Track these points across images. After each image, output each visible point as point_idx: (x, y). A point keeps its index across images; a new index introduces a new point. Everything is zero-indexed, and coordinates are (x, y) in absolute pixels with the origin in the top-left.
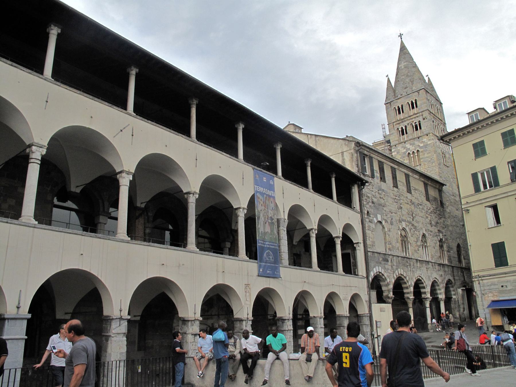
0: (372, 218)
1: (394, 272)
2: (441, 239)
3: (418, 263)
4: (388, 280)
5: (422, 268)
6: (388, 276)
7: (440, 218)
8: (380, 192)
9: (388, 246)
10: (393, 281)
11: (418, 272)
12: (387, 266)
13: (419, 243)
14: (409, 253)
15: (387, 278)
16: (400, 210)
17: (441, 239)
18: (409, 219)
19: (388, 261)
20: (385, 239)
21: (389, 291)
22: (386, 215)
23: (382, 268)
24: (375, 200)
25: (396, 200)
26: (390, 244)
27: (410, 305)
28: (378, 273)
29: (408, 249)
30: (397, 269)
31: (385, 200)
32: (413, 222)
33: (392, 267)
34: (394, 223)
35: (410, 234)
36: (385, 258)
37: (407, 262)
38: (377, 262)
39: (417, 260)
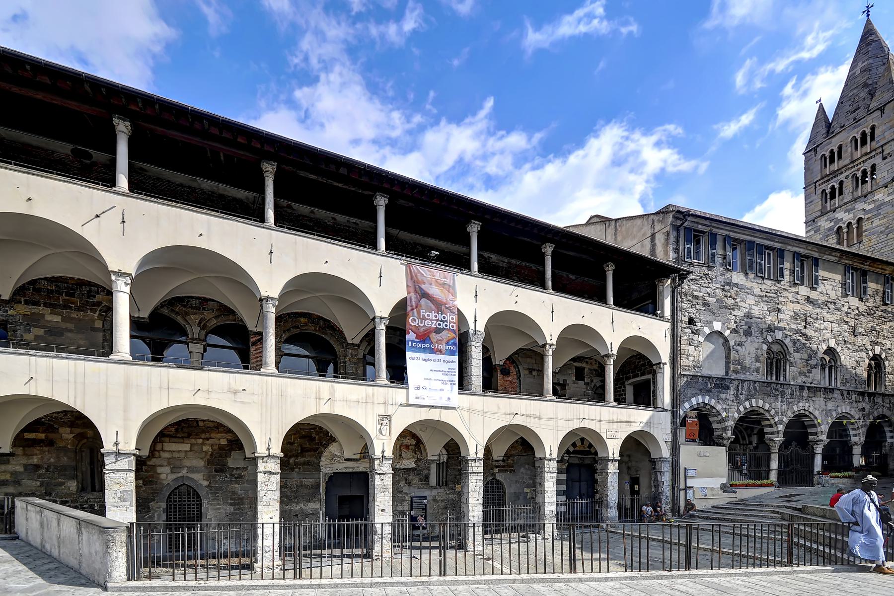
0: (699, 328)
1: (739, 404)
2: (875, 355)
3: (805, 393)
4: (724, 415)
5: (814, 399)
6: (725, 410)
7: (884, 323)
8: (727, 288)
9: (732, 366)
10: (736, 415)
11: (801, 404)
12: (723, 396)
13: (813, 362)
14: (785, 377)
15: (721, 411)
16: (775, 313)
17: (875, 355)
18: (794, 326)
19: (728, 388)
20: (728, 357)
21: (725, 429)
22: (736, 322)
23: (711, 398)
24: (711, 300)
25: (765, 299)
26: (739, 364)
27: (775, 449)
28: (702, 405)
29: (785, 370)
30: (747, 399)
31: (738, 300)
32: (804, 331)
33: (737, 396)
34: (755, 332)
35: (791, 350)
36: (721, 384)
37: (776, 390)
38: (701, 390)
39: (802, 388)
